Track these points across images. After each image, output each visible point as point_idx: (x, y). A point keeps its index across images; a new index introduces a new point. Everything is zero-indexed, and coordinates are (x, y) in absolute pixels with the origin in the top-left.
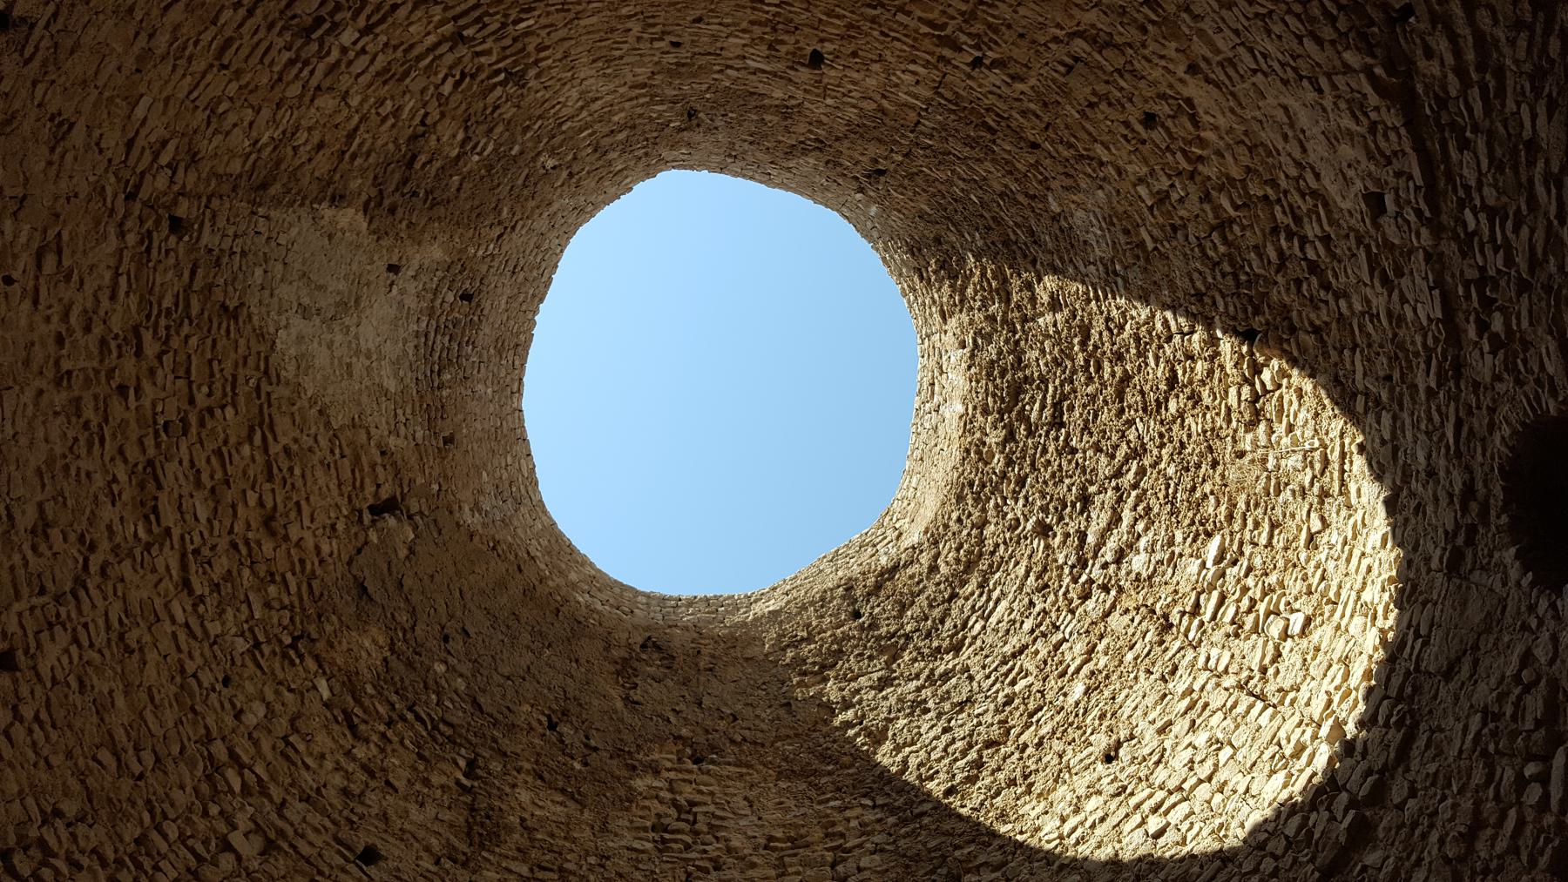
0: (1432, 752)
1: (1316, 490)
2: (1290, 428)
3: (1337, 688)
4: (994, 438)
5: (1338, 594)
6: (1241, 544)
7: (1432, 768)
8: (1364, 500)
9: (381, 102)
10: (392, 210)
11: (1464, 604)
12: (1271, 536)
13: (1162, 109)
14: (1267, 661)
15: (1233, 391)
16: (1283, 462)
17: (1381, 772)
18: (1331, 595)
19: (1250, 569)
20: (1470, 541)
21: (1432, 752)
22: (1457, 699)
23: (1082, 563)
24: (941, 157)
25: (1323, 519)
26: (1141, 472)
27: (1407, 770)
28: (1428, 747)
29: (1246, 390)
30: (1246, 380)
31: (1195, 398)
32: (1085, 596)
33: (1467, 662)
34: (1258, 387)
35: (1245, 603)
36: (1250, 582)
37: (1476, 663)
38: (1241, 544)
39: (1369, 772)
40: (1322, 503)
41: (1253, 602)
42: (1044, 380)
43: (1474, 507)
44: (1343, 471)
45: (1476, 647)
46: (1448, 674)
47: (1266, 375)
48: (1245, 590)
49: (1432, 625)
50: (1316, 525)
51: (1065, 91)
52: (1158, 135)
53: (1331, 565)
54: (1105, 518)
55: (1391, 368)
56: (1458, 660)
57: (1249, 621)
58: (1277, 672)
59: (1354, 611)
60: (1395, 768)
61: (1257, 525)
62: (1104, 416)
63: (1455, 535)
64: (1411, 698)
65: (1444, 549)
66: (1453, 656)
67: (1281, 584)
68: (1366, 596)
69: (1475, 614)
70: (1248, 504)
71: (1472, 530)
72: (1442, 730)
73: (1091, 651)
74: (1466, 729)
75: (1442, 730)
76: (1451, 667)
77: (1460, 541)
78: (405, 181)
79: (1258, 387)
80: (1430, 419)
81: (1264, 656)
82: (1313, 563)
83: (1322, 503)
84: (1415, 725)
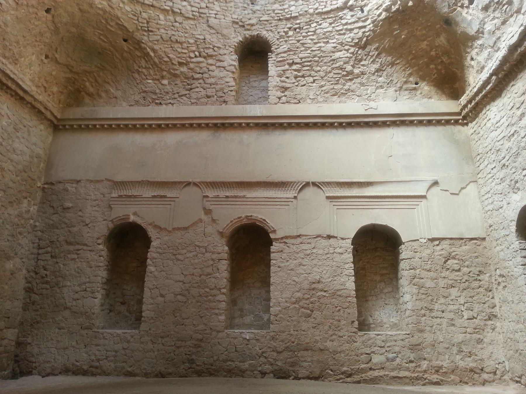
37: (214, 34)
45: (218, 33)
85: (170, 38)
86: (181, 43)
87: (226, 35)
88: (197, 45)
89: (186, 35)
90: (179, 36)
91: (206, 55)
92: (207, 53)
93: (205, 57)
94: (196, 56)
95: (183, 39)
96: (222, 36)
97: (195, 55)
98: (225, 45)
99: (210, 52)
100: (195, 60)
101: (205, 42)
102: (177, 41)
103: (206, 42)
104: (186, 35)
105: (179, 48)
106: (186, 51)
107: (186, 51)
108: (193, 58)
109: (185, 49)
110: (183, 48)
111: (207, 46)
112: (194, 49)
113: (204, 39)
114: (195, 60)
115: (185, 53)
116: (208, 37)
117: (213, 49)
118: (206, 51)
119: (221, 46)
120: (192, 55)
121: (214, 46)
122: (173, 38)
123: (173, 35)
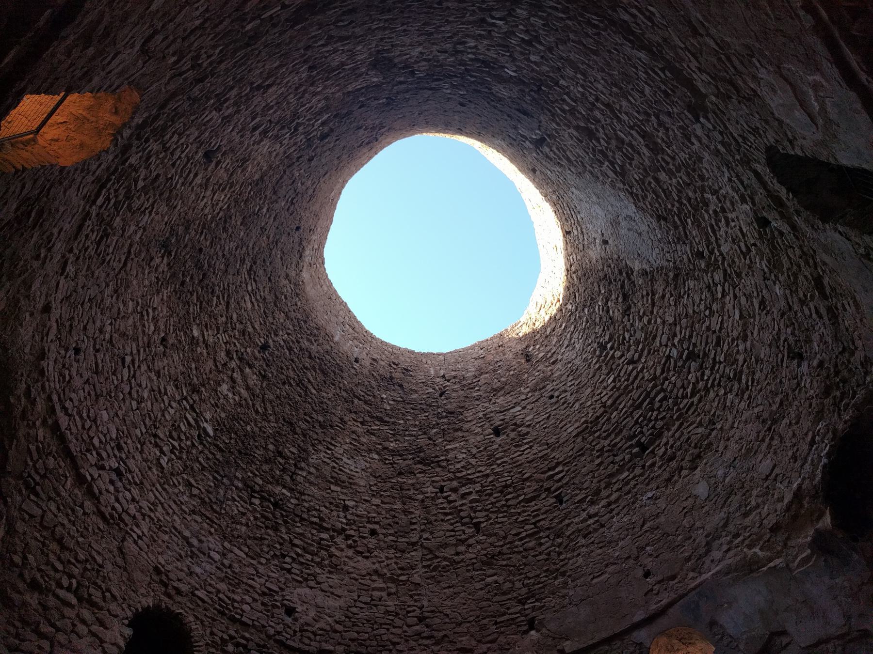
0: (97, 531)
1: (207, 499)
2: (234, 500)
3: (133, 478)
4: (314, 348)
5: (164, 489)
6: (204, 446)
7: (90, 529)
8: (193, 523)
9: (649, 322)
10: (620, 272)
11: (142, 571)
12: (201, 464)
13: (372, 542)
14: (158, 440)
15: (261, 482)
16: (223, 487)
17: (98, 499)
18: (166, 486)
19: (193, 444)
20: (161, 581)
21: (97, 531)
22: (110, 552)
23: (241, 359)
24: (424, 429)
25: (195, 496)
26: (257, 412)
27: (94, 513)
28: (99, 528)
29: (257, 488)
30: (262, 491)
31: (267, 461)
32: (228, 353)
33: (120, 561)
34: (256, 495)
35: (183, 437)
36: (189, 443)
37: (120, 567)
38: (204, 446)
39: (100, 493)
40: (200, 498)
41: (181, 440)
42: (319, 390)
43: (173, 592)
44: (208, 518)
45: (125, 570)
46: (120, 549)
47: (257, 502)
48: (187, 438)
49: (140, 549)
50: (195, 492)
51: (406, 512)
52: (365, 532)
53: (176, 491)
54: (251, 383)
55: (234, 572)
56: (124, 558)
57: (175, 434)
58: (151, 443)
59: (156, 498)
60: (97, 507)
61: (208, 459)
62: (287, 409)
63: (167, 576)
64: (118, 525)
65: (163, 566)
66: (128, 557)
67: (180, 458)
68: (160, 508)
69: (137, 575)
70: (218, 460)
71: (166, 585)
72: (102, 537)
73: (207, 346)
74: (99, 553)
75: (102, 537)
76: (122, 553)
77: (164, 578)
78: (623, 286)
79: (256, 495)
80: (210, 585)
81: (160, 439)
82: (181, 481)
83: (200, 498)
84: (108, 523)
85: (55, 526)
86: (63, 548)
87: (134, 583)
88: (86, 569)
89: (81, 539)
90: (69, 534)
91: (86, 596)
92: (90, 595)
93: (80, 599)
94: (69, 589)
95: (71, 544)
96: (128, 580)
97: (71, 584)
98: (124, 599)
99: (97, 595)
100: (62, 593)
101: (98, 571)
102: (60, 541)
103: (101, 573)
104: (81, 539)
105: (55, 554)
106: (60, 567)
107: (60, 567)
108: (62, 587)
109: (62, 562)
110: (59, 559)
111: (99, 582)
112: (76, 571)
113: (101, 566)
114: (62, 593)
115: (56, 570)
116: (109, 567)
117: (103, 593)
118: (92, 590)
119: (118, 597)
120: (65, 582)
121: (109, 590)
122: (59, 529)
123: (63, 525)
